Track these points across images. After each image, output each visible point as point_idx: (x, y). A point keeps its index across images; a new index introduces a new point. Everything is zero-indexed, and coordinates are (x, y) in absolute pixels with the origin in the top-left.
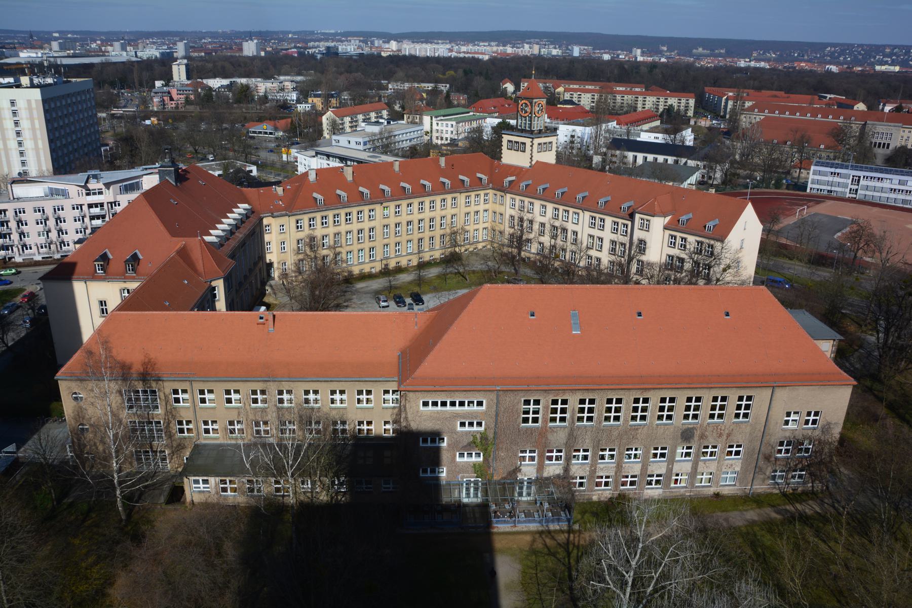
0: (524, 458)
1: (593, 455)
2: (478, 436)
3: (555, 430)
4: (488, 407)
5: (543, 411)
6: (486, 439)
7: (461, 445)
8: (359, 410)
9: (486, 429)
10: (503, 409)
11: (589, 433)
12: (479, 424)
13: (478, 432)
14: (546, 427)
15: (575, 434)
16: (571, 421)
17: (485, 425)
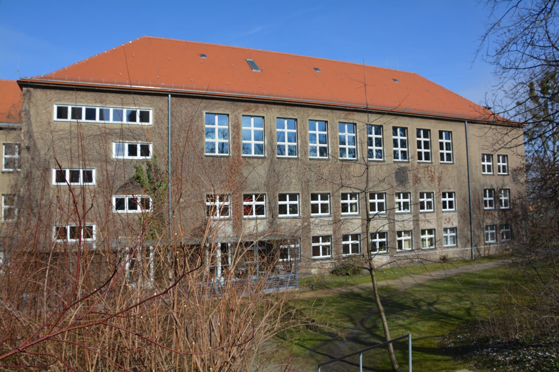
0: (210, 210)
1: (303, 204)
2: (144, 167)
3: (251, 161)
4: (156, 122)
5: (233, 131)
6: (157, 171)
7: (118, 184)
8: (6, 174)
9: (155, 157)
10: (178, 126)
11: (294, 168)
12: (145, 151)
13: (142, 161)
14: (239, 156)
15: (277, 170)
16: (270, 149)
17: (154, 149)
